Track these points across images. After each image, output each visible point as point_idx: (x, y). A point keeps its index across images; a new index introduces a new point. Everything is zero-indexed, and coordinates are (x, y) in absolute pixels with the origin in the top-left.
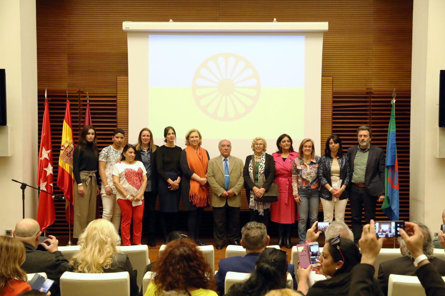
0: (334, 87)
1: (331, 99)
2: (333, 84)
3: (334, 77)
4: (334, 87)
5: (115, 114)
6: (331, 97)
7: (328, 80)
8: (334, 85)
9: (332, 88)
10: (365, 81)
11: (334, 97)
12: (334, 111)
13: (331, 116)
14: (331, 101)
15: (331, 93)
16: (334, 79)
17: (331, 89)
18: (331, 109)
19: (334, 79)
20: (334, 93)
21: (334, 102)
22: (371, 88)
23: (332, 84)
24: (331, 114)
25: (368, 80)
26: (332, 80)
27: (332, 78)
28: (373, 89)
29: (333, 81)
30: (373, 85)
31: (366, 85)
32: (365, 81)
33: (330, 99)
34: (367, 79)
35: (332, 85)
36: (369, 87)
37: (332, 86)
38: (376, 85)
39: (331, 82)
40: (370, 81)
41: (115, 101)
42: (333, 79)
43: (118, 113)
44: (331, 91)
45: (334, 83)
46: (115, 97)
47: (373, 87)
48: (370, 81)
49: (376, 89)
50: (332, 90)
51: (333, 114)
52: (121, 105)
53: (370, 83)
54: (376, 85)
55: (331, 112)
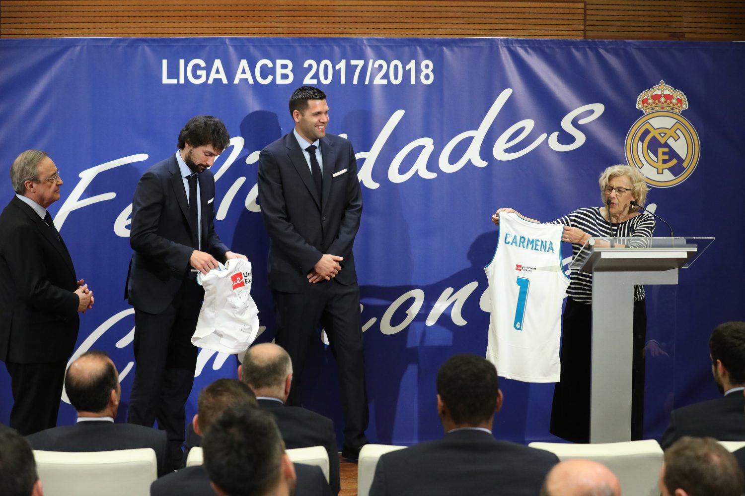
0: (588, 28)
2: (585, 20)
4: (588, 28)
7: (573, 11)
8: (588, 23)
9: (585, 31)
10: (666, 14)
16: (588, 7)
17: (582, 32)
22: (683, 34)
23: (582, 22)
25: (673, 13)
26: (582, 11)
27: (582, 5)
28: (687, 35)
29: (585, 14)
30: (685, 24)
31: (670, 25)
32: (666, 14)
34: (670, 9)
35: (585, 25)
36: (678, 30)
37: (582, 27)
38: (693, 25)
39: (582, 17)
40: (678, 14)
42: (585, 9)
45: (588, 17)
47: (685, 30)
48: (678, 14)
49: (694, 36)
50: (585, 36)
53: (680, 19)
54: (693, 25)
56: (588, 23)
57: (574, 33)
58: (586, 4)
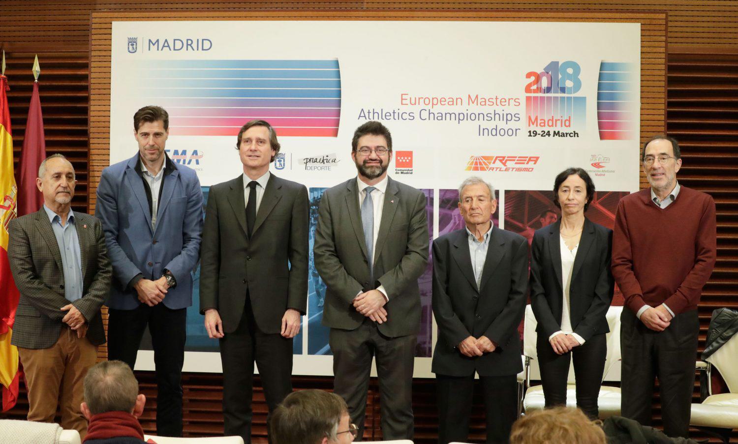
0: (670, 40)
1: (663, 73)
2: (666, 30)
3: (670, 13)
4: (670, 40)
5: (85, 111)
6: (663, 67)
7: (654, 22)
9: (666, 42)
11: (670, 69)
12: (670, 104)
13: (663, 118)
14: (663, 78)
15: (663, 56)
16: (670, 18)
17: (663, 44)
18: (663, 101)
19: (670, 18)
20: (671, 57)
21: (671, 81)
23: (664, 33)
24: (663, 112)
26: (663, 22)
27: (663, 16)
29: (666, 24)
33: (661, 72)
35: (666, 36)
37: (664, 38)
39: (663, 28)
41: (85, 78)
42: (666, 19)
43: (92, 108)
44: (663, 50)
46: (86, 66)
50: (666, 47)
51: (670, 115)
52: (100, 86)
55: (663, 106)
56: (669, 34)
57: (656, 44)
58: (667, 14)
